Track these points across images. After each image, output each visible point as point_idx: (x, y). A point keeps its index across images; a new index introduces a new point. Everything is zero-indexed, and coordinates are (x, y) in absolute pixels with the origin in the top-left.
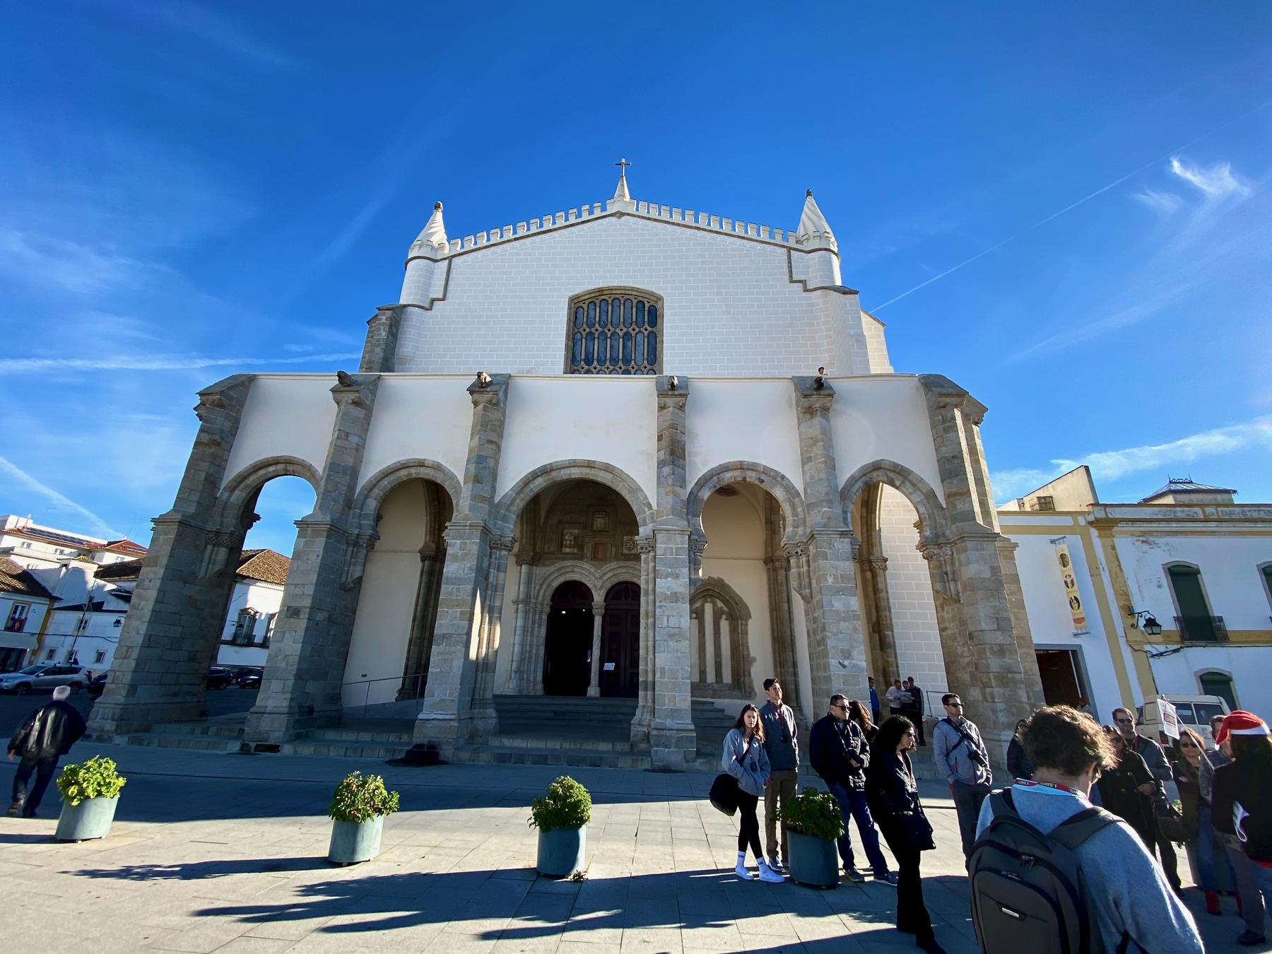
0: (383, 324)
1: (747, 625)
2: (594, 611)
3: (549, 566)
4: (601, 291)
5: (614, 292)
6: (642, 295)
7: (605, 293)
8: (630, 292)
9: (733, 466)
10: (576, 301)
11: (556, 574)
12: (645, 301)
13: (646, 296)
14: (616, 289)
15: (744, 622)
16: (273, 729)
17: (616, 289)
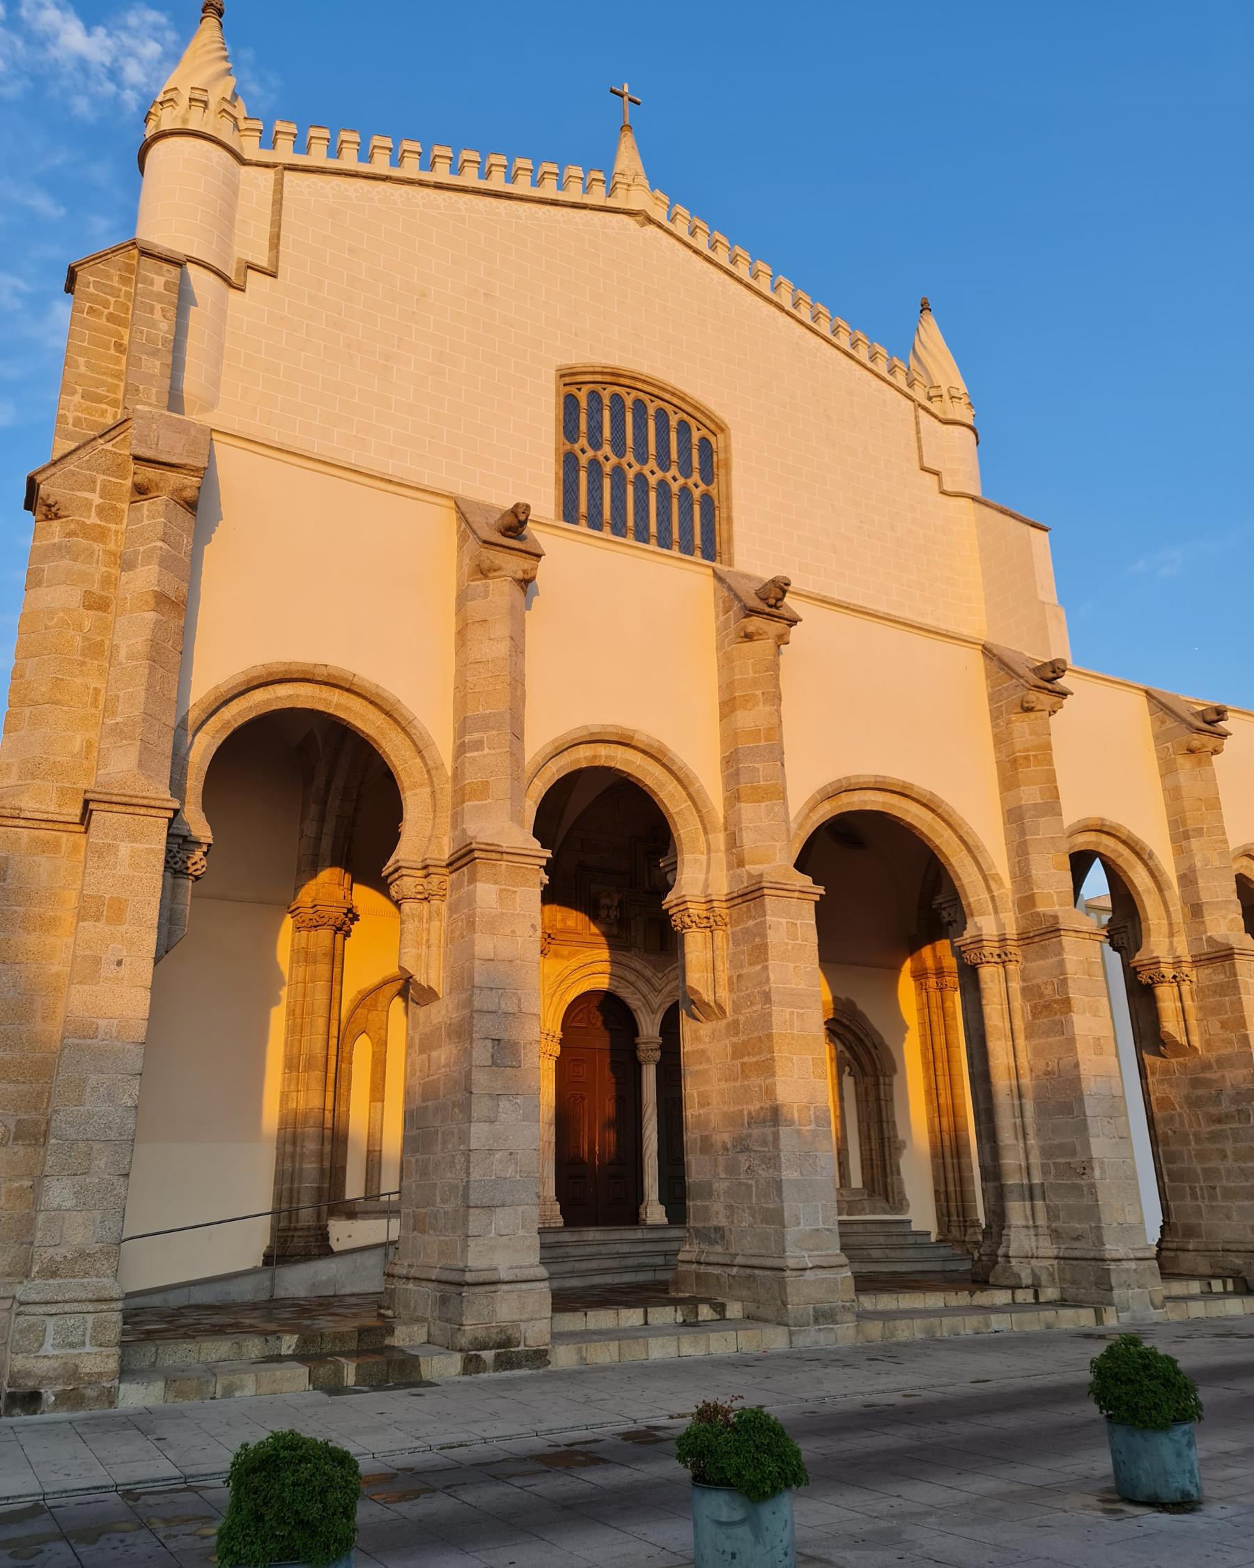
0: (159, 297)
1: (891, 1085)
2: (641, 1055)
3: (568, 958)
4: (615, 376)
5: (640, 385)
6: (690, 410)
7: (623, 381)
8: (667, 396)
9: (680, 768)
10: (568, 380)
11: (576, 976)
12: (693, 423)
13: (698, 415)
14: (644, 381)
15: (887, 1080)
16: (524, 1317)
17: (644, 381)
